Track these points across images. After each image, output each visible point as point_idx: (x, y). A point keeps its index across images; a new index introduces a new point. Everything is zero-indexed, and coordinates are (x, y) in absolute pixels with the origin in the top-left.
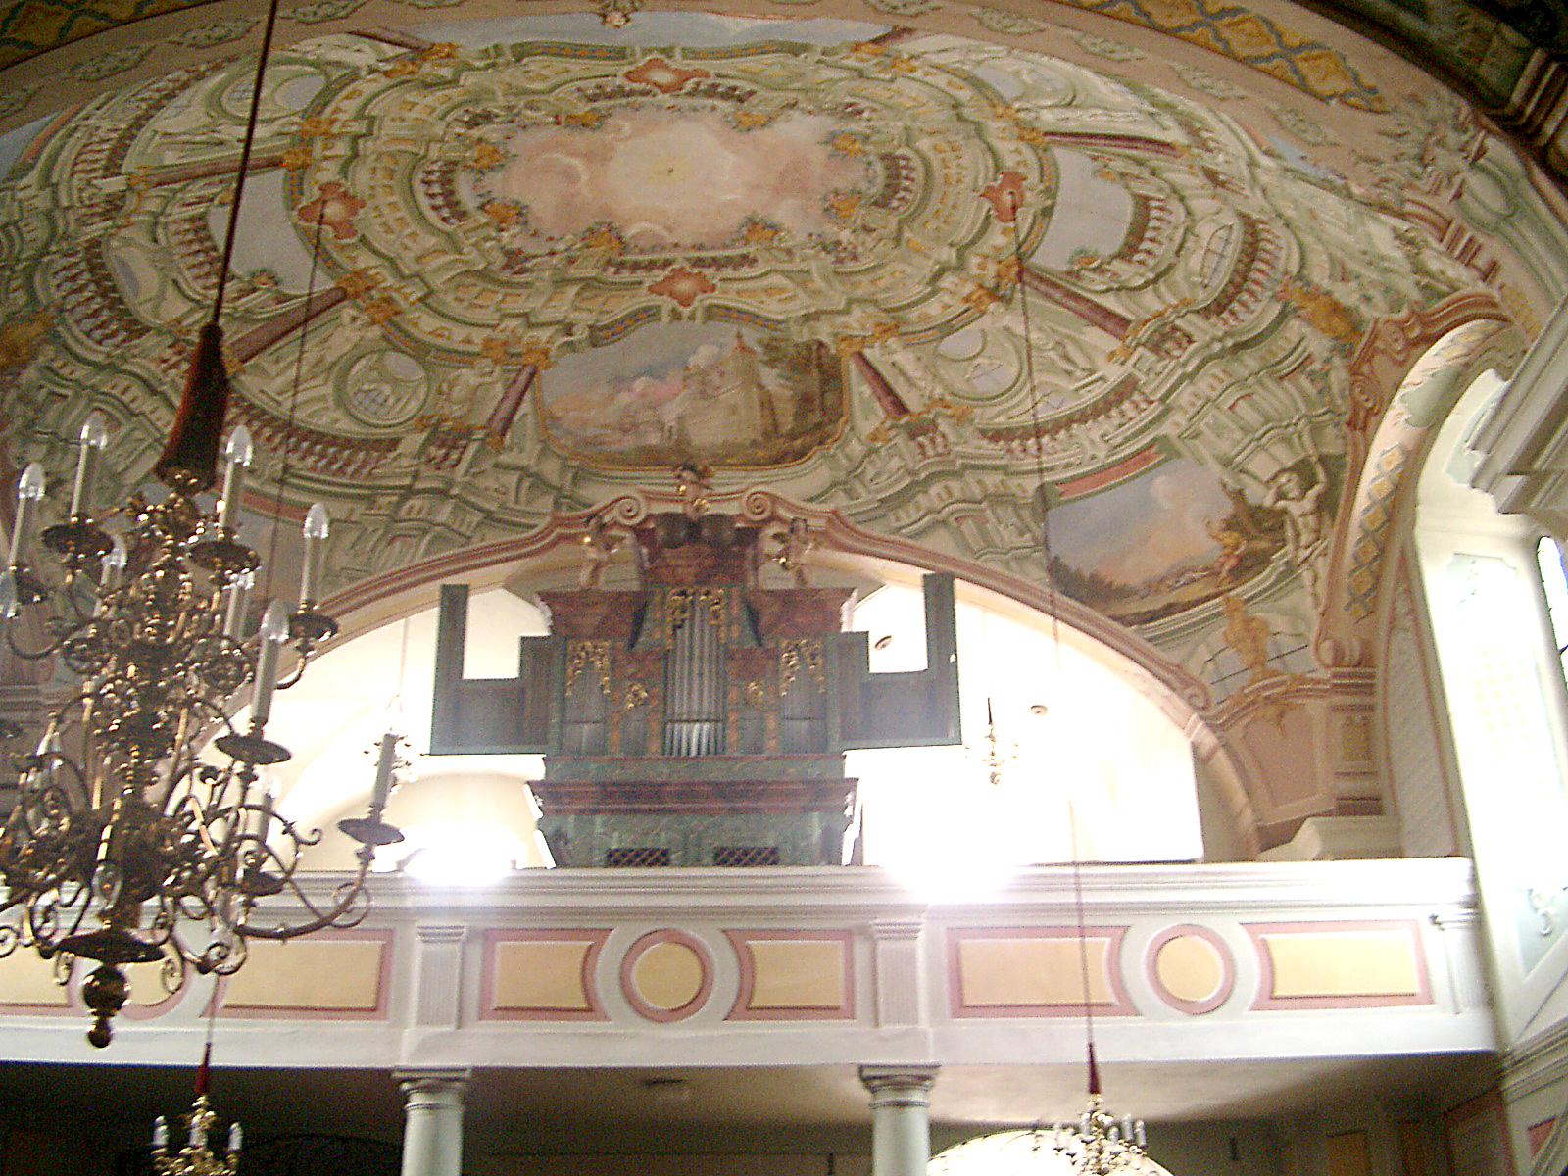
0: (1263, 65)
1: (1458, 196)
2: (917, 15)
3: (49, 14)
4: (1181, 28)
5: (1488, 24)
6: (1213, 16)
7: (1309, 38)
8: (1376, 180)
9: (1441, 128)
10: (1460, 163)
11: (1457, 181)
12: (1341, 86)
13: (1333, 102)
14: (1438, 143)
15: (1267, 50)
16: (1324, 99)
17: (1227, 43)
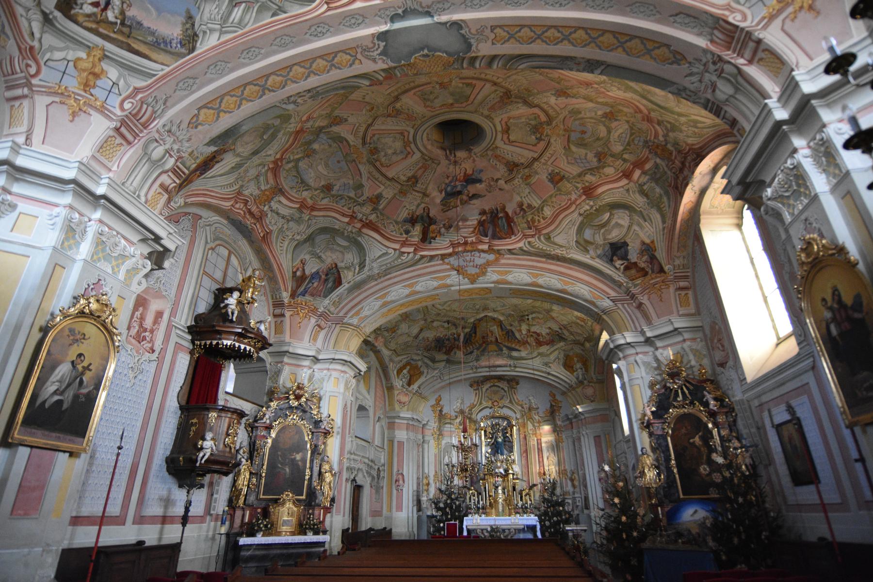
0: (219, 100)
1: (157, 141)
2: (310, 27)
3: (603, 43)
4: (245, 89)
5: (198, 161)
6: (241, 100)
7: (220, 119)
8: (157, 98)
9: (179, 144)
10: (167, 146)
11: (161, 142)
12: (201, 118)
13: (196, 112)
14: (174, 140)
15: (223, 105)
16: (199, 109)
17: (232, 96)
